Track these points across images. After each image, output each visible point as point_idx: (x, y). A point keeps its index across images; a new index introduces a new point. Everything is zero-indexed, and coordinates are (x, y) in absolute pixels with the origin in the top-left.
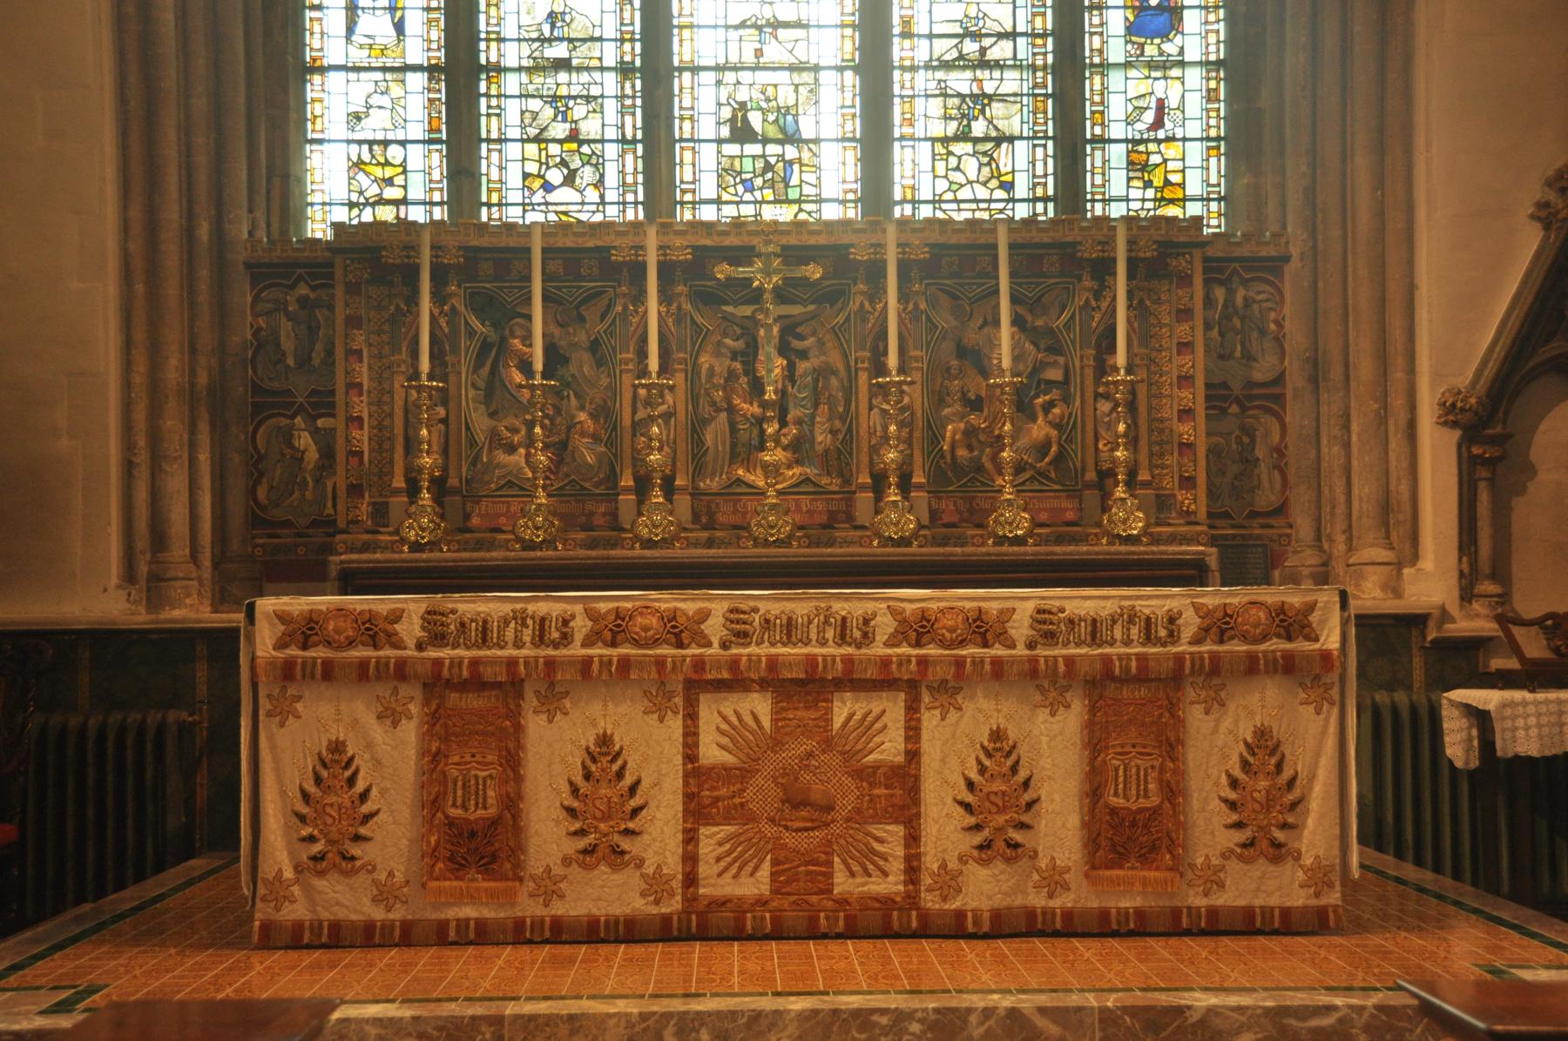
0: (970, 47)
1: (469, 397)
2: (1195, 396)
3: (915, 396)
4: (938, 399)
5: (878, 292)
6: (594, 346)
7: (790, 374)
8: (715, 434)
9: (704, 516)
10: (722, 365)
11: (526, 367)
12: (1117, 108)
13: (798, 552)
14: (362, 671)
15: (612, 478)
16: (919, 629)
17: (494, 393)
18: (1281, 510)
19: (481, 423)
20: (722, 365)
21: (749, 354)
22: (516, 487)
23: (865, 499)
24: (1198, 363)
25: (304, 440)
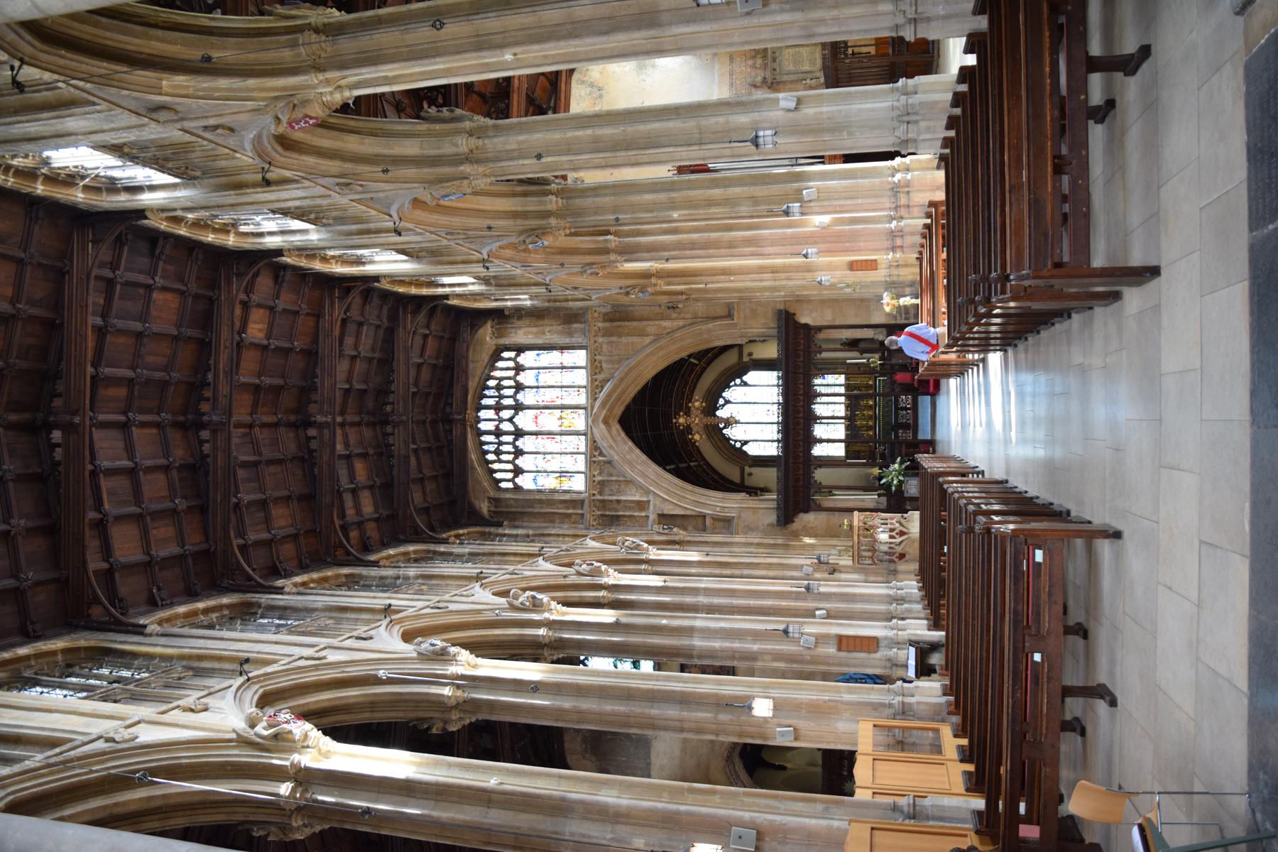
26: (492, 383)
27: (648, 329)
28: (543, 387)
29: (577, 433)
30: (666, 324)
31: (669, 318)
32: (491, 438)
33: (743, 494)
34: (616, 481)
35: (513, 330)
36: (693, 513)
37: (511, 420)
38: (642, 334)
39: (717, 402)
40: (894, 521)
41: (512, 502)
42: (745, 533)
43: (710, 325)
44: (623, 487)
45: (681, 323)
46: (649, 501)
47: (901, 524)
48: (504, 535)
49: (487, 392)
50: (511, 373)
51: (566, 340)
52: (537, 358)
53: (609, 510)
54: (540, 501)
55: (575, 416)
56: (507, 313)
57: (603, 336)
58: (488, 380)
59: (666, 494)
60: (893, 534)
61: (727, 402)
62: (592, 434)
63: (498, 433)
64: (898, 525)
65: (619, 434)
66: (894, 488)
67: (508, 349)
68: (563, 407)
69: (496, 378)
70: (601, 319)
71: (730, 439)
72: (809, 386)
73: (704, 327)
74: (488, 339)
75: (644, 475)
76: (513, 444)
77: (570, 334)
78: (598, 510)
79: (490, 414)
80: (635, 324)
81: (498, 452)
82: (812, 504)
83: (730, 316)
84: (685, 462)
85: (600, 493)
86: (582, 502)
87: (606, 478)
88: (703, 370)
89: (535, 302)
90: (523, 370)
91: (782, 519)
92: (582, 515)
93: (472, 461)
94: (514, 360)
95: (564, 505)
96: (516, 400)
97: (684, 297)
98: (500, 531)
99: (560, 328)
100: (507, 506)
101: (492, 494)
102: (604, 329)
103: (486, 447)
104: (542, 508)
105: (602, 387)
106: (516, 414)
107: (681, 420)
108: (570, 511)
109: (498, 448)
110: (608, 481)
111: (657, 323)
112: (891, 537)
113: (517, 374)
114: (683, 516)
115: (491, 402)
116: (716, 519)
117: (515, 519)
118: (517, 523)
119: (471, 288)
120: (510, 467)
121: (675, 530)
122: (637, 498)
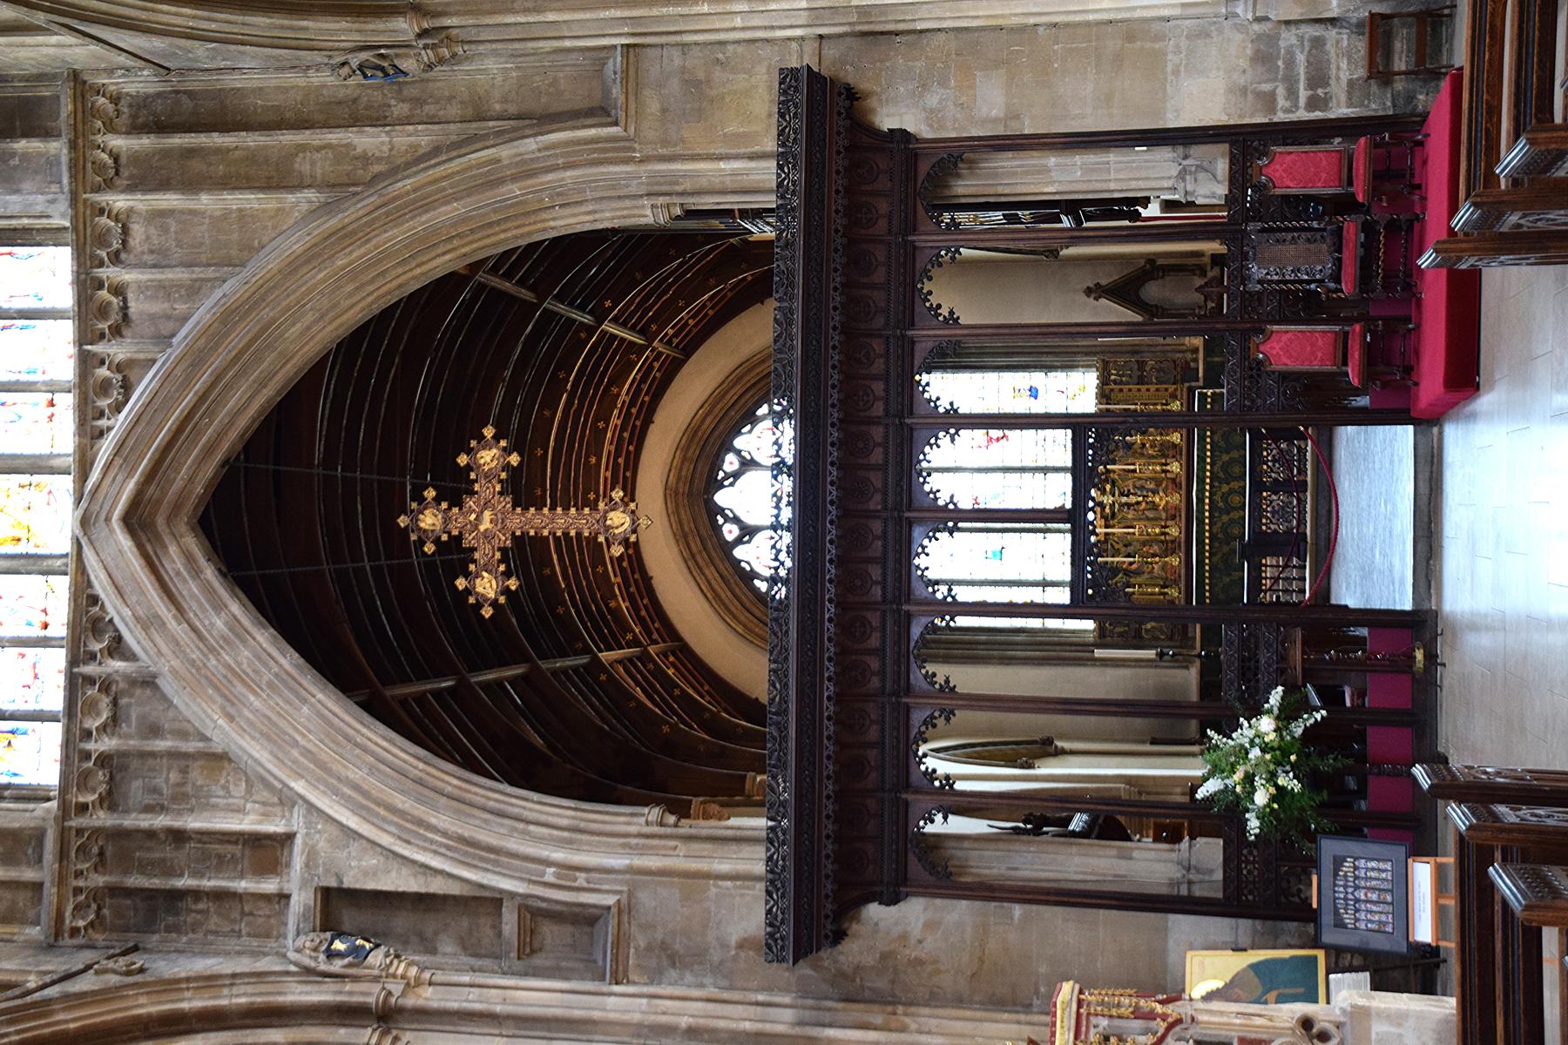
0: (1040, 444)
1: (1139, 580)
2: (1144, 387)
3: (1142, 461)
4: (1142, 455)
6: (1125, 546)
7: (1134, 494)
8: (1150, 514)
9: (1173, 518)
10: (1131, 512)
11: (1131, 564)
13: (1183, 492)
15: (1162, 542)
17: (1138, 573)
18: (1174, 361)
20: (1131, 512)
21: (1129, 505)
22: (1164, 568)
23: (1169, 475)
25: (1149, 626)
27: (302, 165)
30: (367, 140)
31: (377, 119)
33: (654, 813)
34: (174, 755)
36: (454, 889)
38: (277, 177)
39: (717, 464)
42: (655, 976)
43: (530, 145)
44: (197, 775)
45: (421, 137)
46: (289, 837)
53: (144, 868)
59: (357, 810)
61: (748, 464)
62: (81, 572)
65: (196, 573)
66: (1253, 824)
70: (123, 121)
71: (753, 575)
72: (909, 391)
73: (505, 152)
75: (273, 737)
78: (101, 864)
80: (252, 140)
82: (915, 867)
84: (586, 650)
85: (110, 801)
86: (39, 836)
88: (672, 369)
91: (787, 930)
92: (37, 887)
102: (136, 159)
105: (127, 388)
107: (430, 520)
110: (144, 755)
116: (535, 915)
121: (377, 958)
122: (247, 823)
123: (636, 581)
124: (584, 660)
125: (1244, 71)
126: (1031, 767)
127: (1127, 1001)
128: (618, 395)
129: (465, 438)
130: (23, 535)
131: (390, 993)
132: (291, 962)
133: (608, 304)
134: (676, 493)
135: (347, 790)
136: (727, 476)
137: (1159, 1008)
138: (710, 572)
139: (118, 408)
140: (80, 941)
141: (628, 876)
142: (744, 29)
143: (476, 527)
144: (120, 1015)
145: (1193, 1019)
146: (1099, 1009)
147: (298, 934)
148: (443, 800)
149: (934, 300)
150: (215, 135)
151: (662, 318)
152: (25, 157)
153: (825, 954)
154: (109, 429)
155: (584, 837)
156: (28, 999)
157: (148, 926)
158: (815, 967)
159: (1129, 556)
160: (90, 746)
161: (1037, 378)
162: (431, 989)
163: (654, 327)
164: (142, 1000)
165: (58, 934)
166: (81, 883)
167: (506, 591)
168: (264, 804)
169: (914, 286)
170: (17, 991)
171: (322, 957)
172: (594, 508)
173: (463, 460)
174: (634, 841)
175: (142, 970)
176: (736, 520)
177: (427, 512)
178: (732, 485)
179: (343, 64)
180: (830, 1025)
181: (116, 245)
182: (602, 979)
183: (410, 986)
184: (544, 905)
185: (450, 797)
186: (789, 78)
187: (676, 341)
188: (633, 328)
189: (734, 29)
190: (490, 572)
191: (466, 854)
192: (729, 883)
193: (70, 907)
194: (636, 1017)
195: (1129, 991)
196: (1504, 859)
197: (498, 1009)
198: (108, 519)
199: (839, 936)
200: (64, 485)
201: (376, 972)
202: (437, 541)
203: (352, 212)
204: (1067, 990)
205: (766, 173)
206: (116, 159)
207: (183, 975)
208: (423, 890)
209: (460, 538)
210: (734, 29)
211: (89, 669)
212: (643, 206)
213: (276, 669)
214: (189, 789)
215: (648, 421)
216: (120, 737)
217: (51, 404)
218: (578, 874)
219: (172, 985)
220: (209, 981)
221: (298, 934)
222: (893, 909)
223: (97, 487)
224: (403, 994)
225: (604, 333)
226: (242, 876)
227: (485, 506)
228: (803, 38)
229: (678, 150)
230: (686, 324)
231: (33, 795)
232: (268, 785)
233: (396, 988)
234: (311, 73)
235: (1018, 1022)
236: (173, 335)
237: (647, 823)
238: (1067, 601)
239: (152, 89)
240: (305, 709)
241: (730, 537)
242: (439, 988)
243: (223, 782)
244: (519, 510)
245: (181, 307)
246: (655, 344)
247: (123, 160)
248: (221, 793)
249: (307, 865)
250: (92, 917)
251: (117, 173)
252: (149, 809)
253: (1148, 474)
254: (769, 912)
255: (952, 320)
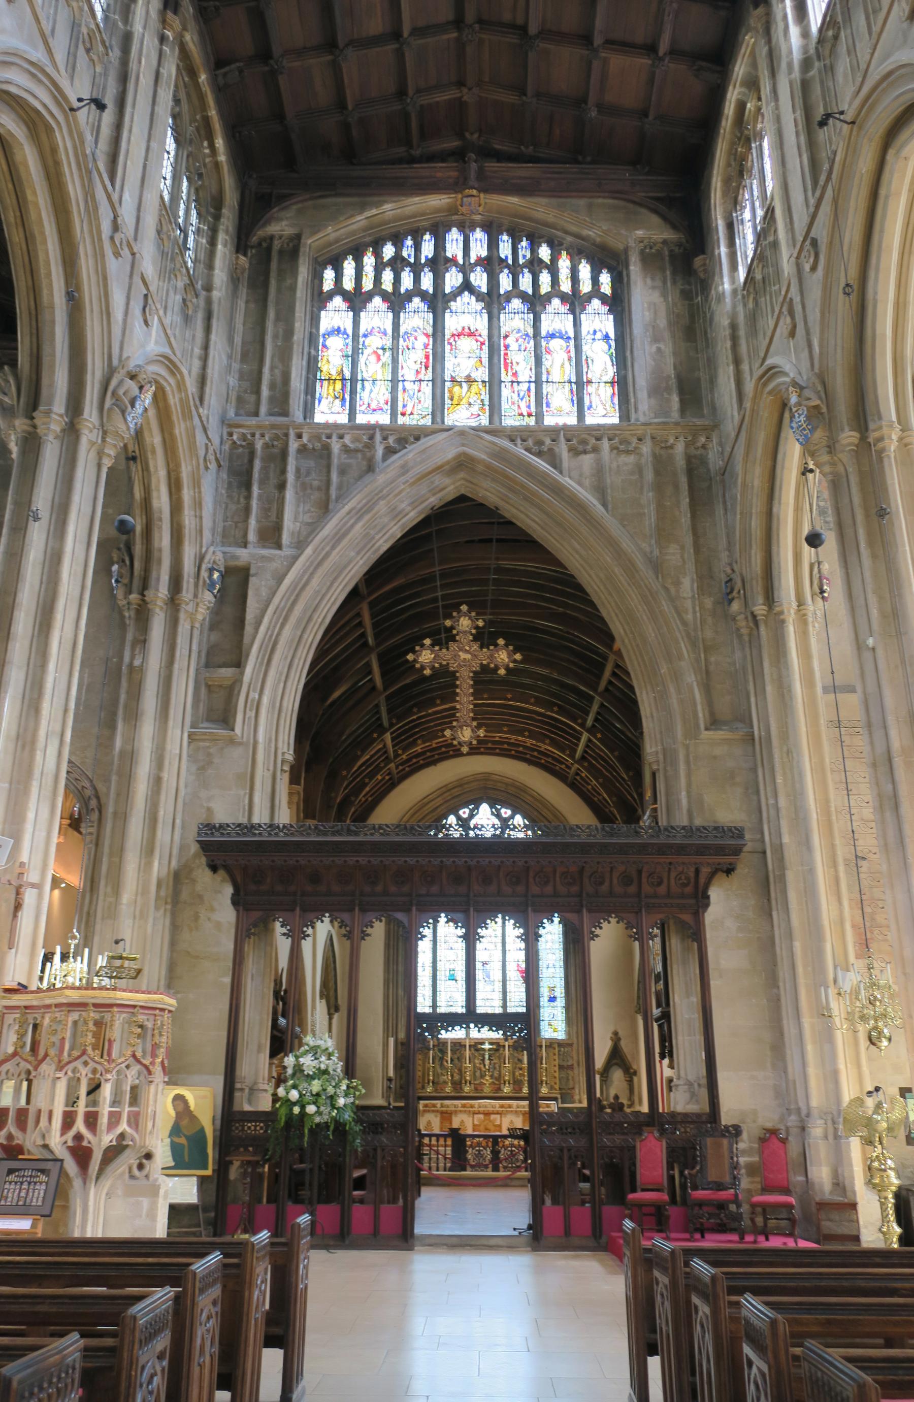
2: (557, 1069)
5: (504, 1050)
6: (458, 1058)
8: (478, 1074)
9: (476, 1089)
12: (546, 1015)
14: (433, 1111)
16: (502, 1106)
17: (442, 1065)
18: (573, 1088)
19: (440, 1071)
21: (483, 1060)
22: (445, 1083)
24: (557, 1063)
26: (544, 252)
27: (673, 549)
28: (537, 346)
29: (438, 408)
30: (687, 585)
32: (428, 249)
33: (290, 757)
34: (328, 483)
35: (658, 283)
36: (246, 640)
37: (467, 286)
38: (663, 534)
39: (505, 804)
40: (123, 1126)
41: (289, 282)
42: (192, 758)
43: (691, 678)
44: (316, 496)
46: (279, 546)
47: (113, 1153)
48: (212, 242)
49: (524, 243)
50: (566, 286)
51: (641, 379)
52: (599, 335)
53: (265, 470)
54: (289, 333)
55: (475, 409)
56: (698, 261)
57: (655, 456)
58: (551, 245)
59: (294, 584)
60: (80, 1125)
62: (435, 432)
63: (439, 263)
64: (107, 1139)
67: (618, 281)
68: (494, 385)
69: (554, 259)
70: (692, 451)
74: (640, 233)
75: (338, 537)
76: (417, 291)
77: (655, 391)
78: (266, 446)
79: (479, 249)
80: (685, 520)
81: (397, 264)
83: (714, 723)
84: (392, 725)
86: (285, 413)
87: (335, 461)
88: (561, 776)
89: (728, 300)
90: (572, 311)
91: (217, 838)
92: (256, 414)
93: (378, 205)
94: (596, 292)
95: (279, 380)
96: (508, 297)
97: (760, 609)
98: (222, 250)
99: (670, 371)
100: (281, 273)
101: (310, 242)
103: (409, 242)
104: (275, 336)
105: (539, 454)
106: (479, 297)
107: (465, 623)
108: (265, 392)
109: (404, 262)
111: (691, 566)
112: (68, 1120)
113: (564, 298)
114: (240, 622)
115: (505, 249)
117: (252, 285)
118: (243, 292)
119: (794, 31)
120: (368, 284)
121: (208, 597)
123: (433, 756)
124: (386, 723)
125: (754, 1122)
126: (321, 997)
127: (164, 1039)
128: (545, 744)
129: (516, 641)
130: (455, 401)
131: (187, 604)
132: (207, 549)
133: (599, 736)
134: (486, 780)
135: (306, 577)
136: (498, 811)
137: (158, 1060)
138: (439, 801)
139: (528, 450)
140: (225, 436)
141: (252, 741)
142: (767, 805)
143: (461, 650)
144: (182, 456)
145: (151, 1082)
146: (159, 1022)
147: (224, 553)
148: (299, 633)
149: (605, 925)
150: (688, 500)
151: (591, 769)
152: (668, 401)
153: (204, 860)
154: (516, 445)
155: (276, 716)
156: (193, 408)
157: (232, 472)
158: (196, 856)
159: (452, 1060)
160: (334, 438)
161: (561, 1002)
162: (189, 627)
163: (586, 764)
164: (189, 468)
165: (230, 426)
166: (257, 436)
167: (423, 668)
168: (299, 533)
169: (613, 912)
170: (198, 403)
171: (210, 566)
172: (474, 719)
173: (501, 642)
174: (273, 745)
175: (207, 468)
176: (471, 816)
177: (470, 622)
178: (493, 814)
179: (733, 570)
180: (160, 863)
181: (622, 447)
182: (192, 727)
183: (192, 617)
184: (236, 692)
185: (301, 637)
186: (738, 833)
187: (578, 778)
188: (585, 752)
189: (767, 799)
190: (434, 658)
191: (267, 646)
192: (247, 801)
193: (244, 431)
194: (168, 747)
195: (170, 1042)
196: (225, 1266)
197: (176, 666)
198: (463, 445)
199: (214, 868)
200: (484, 421)
201: (200, 596)
202: (452, 628)
203: (646, 572)
204: (170, 1002)
205: (682, 820)
206: (671, 447)
207: (203, 490)
208: (247, 622)
209: (454, 640)
210: (767, 799)
211: (378, 437)
212: (657, 746)
213: (377, 537)
214: (309, 491)
215: (530, 762)
216: (339, 454)
217: (530, 415)
218: (254, 712)
219: (196, 484)
220: (198, 504)
221: (224, 553)
222: (229, 902)
223: (481, 438)
224: (186, 611)
225: (581, 734)
226: (258, 521)
227: (475, 656)
228: (763, 841)
229: (693, 767)
230: (589, 784)
231: (309, 410)
232: (310, 534)
233: (190, 607)
234: (727, 553)
235: (159, 980)
236: (570, 477)
237: (283, 753)
238: (420, 1010)
239: (711, 466)
240: (353, 554)
241: (461, 812)
242: (189, 632)
243: (312, 509)
244: (471, 675)
245: (587, 482)
246: (576, 766)
247: (670, 451)
248: (306, 509)
249: (263, 557)
250: (238, 443)
251: (662, 448)
252: (298, 470)
253: (503, 1072)
254: (228, 826)
255: (594, 936)
